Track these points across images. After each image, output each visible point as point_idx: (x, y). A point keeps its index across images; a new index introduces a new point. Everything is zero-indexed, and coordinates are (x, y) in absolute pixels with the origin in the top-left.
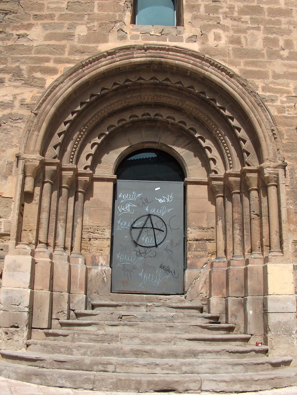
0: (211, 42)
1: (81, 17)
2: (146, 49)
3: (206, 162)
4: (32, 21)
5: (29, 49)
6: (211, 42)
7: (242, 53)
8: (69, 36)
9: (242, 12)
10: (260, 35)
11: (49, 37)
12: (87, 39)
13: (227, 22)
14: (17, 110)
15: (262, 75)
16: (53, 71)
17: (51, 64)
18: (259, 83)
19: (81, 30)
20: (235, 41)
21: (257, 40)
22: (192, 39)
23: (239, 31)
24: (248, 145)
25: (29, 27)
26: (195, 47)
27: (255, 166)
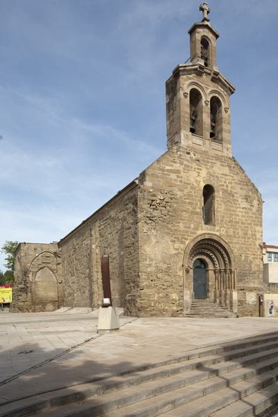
0: (222, 232)
1: (191, 221)
2: (208, 234)
3: (214, 264)
4: (180, 221)
5: (180, 231)
6: (222, 232)
7: (228, 236)
8: (189, 228)
9: (229, 222)
10: (232, 230)
11: (185, 227)
12: (194, 229)
13: (225, 226)
14: (180, 251)
15: (232, 243)
16: (187, 239)
17: (186, 237)
18: (231, 245)
19: (192, 226)
20: (227, 232)
21: (231, 232)
22: (218, 231)
23: (228, 229)
24: (227, 262)
25: (179, 223)
26: (218, 234)
27: (229, 268)
